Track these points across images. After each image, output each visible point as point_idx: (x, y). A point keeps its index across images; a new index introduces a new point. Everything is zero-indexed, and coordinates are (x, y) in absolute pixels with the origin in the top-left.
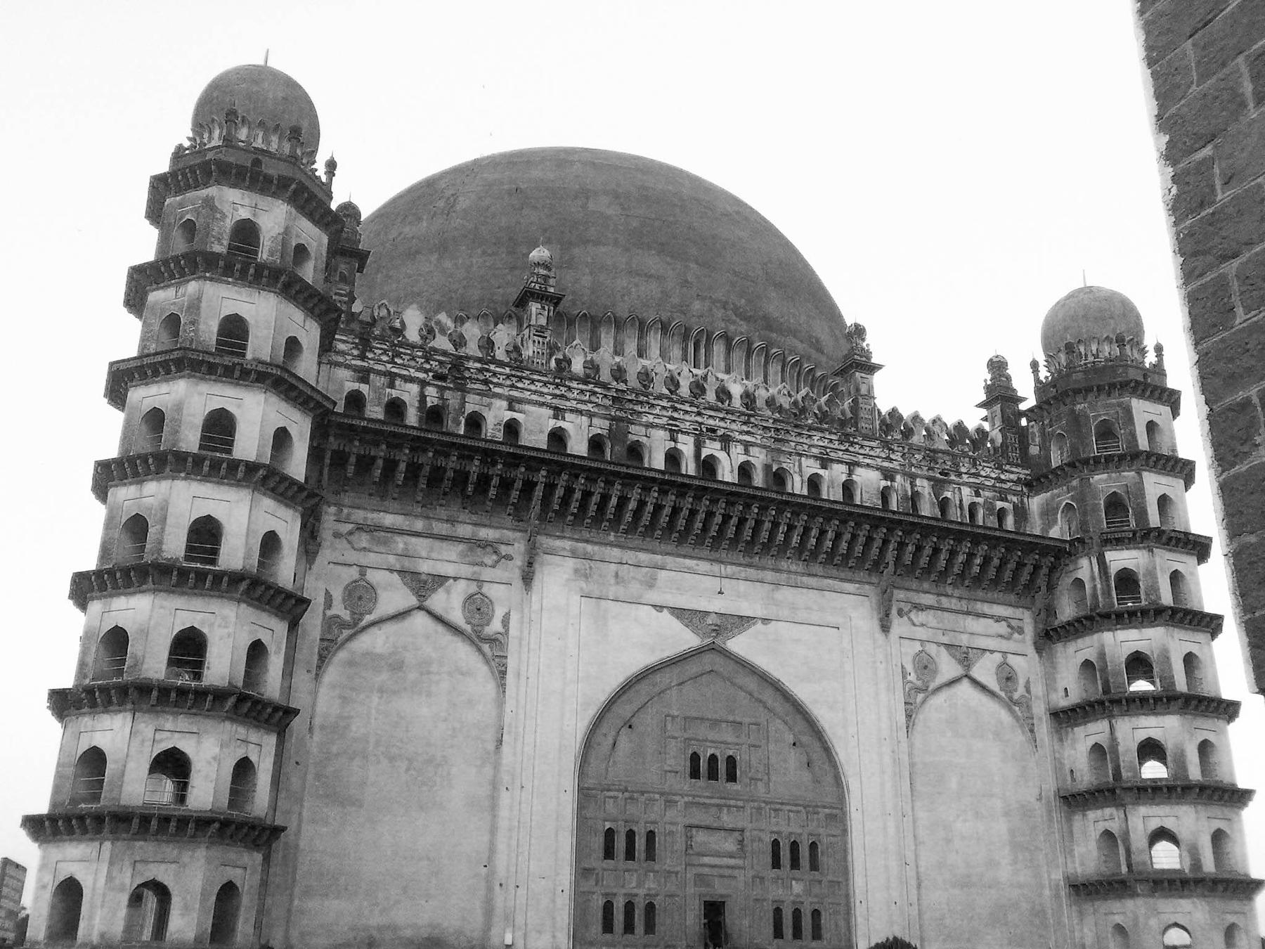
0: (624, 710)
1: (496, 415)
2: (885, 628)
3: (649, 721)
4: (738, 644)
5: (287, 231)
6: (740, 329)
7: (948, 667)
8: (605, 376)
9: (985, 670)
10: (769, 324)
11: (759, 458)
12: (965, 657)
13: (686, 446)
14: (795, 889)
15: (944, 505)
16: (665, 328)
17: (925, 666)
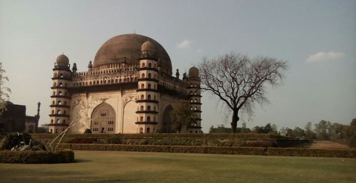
0: (95, 110)
1: (85, 81)
2: (122, 96)
3: (98, 111)
4: (107, 102)
5: (59, 73)
6: (113, 62)
7: (129, 99)
8: (95, 74)
9: (133, 99)
10: (118, 59)
11: (110, 79)
12: (131, 98)
13: (103, 80)
14: (111, 126)
15: (132, 79)
16: (105, 65)
17: (126, 100)
